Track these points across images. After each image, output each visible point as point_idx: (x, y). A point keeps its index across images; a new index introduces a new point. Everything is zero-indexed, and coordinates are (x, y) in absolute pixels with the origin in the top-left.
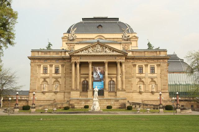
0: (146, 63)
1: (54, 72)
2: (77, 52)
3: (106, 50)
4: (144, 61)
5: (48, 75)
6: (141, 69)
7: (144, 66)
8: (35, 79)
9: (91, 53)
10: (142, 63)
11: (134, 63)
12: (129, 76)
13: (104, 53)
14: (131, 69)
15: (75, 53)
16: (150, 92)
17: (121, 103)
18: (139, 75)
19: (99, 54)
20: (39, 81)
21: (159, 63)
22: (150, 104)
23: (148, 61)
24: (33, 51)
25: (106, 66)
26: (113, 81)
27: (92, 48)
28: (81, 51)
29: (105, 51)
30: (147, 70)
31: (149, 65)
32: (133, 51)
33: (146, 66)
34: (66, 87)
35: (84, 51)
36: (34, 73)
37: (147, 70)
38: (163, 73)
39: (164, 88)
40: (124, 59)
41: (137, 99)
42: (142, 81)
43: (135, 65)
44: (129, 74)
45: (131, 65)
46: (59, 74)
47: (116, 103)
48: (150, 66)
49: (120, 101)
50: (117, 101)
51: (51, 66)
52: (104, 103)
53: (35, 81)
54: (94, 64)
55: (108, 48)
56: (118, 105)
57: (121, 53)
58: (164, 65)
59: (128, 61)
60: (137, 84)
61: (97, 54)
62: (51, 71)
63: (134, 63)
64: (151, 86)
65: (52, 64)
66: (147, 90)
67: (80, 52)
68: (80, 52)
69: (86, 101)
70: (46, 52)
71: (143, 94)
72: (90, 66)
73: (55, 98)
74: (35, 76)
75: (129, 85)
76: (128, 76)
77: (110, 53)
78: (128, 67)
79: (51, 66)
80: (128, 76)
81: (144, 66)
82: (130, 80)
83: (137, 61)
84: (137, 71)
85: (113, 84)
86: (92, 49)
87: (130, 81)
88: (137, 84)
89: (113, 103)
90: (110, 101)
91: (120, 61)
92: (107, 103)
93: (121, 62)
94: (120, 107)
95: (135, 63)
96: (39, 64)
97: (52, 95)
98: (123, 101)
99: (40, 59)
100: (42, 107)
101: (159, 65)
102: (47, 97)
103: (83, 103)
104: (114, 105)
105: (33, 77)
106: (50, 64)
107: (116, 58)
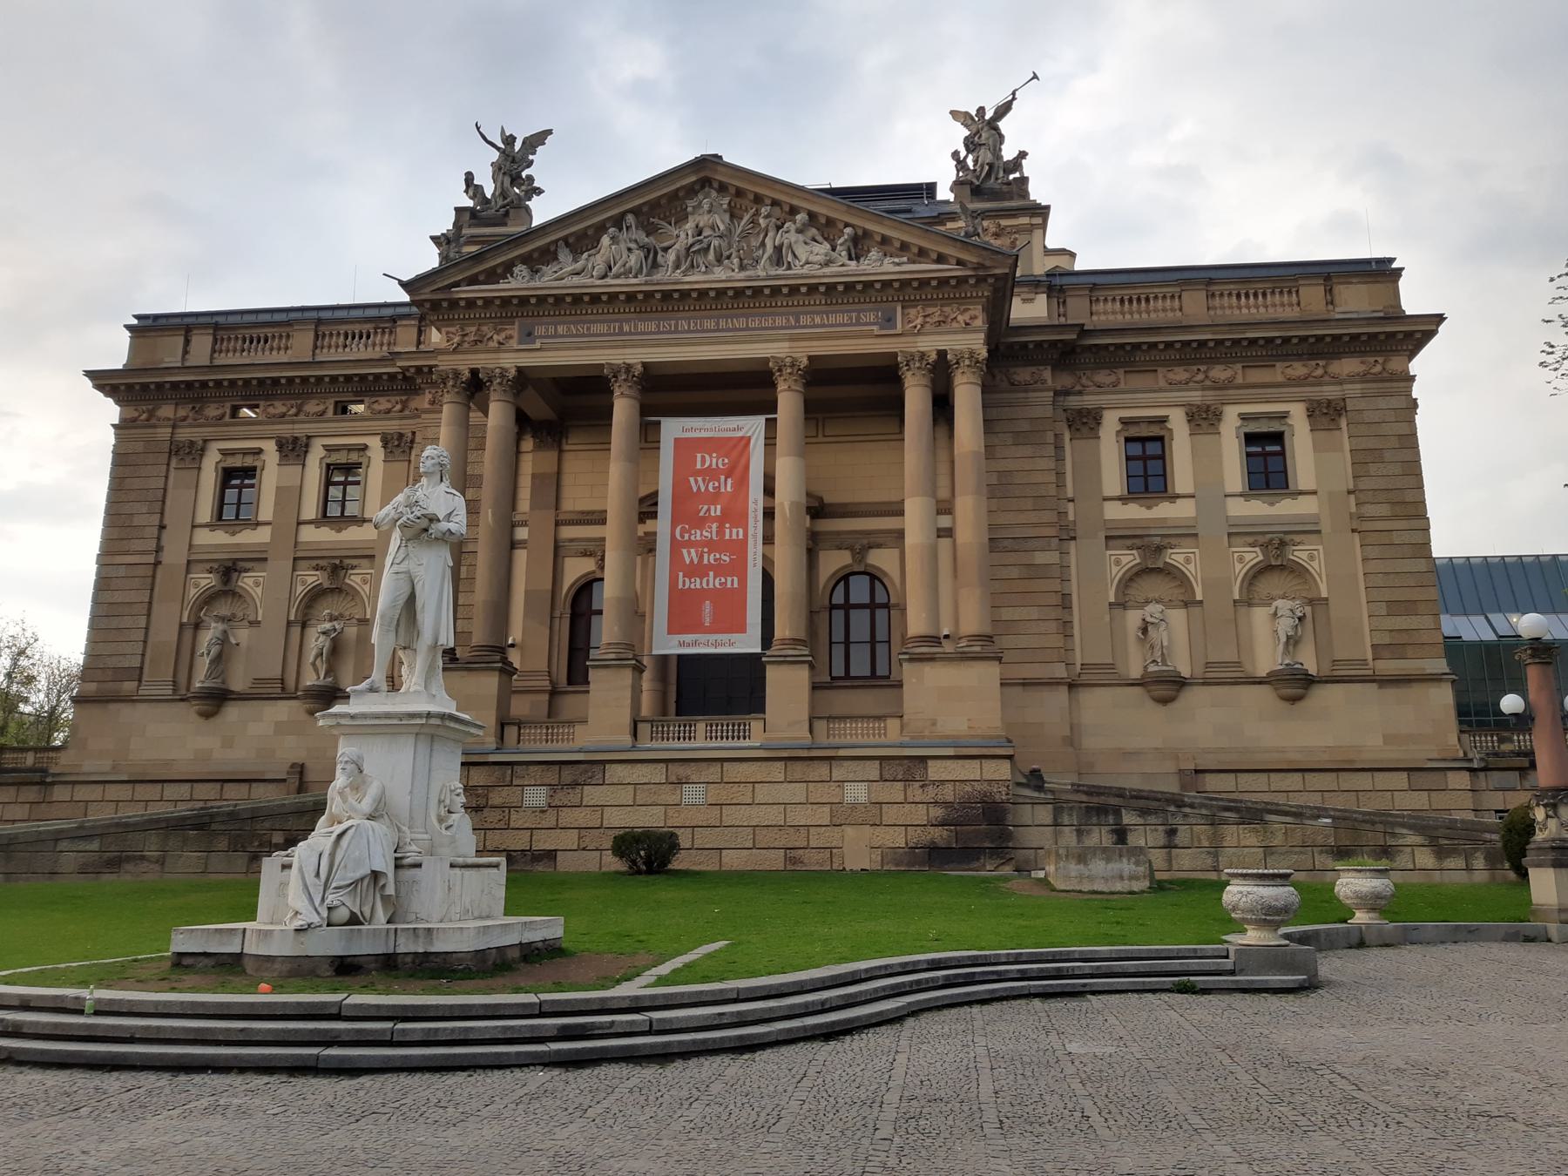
0: (1195, 397)
1: (310, 510)
2: (492, 276)
3: (790, 236)
4: (1180, 374)
5: (262, 536)
6: (1148, 467)
7: (1178, 422)
8: (141, 571)
9: (626, 274)
10: (1164, 401)
11: (1074, 402)
12: (1033, 517)
13: (763, 273)
14: (1051, 450)
15: (473, 280)
16: (1260, 682)
17: (948, 794)
18: (1135, 512)
19: (722, 276)
21: (1330, 392)
22: (1296, 801)
23: (1219, 373)
24: (147, 328)
25: (788, 402)
26: (874, 577)
27: (651, 230)
28: (526, 260)
29: (778, 249)
30: (1208, 464)
31: (1231, 414)
32: (1062, 289)
33: (1204, 419)
35: (564, 255)
36: (137, 521)
37: (1208, 464)
38: (1382, 483)
39: (1404, 638)
40: (979, 322)
41: (1127, 755)
42: (1169, 572)
43: (1085, 422)
44: (1029, 504)
45: (1048, 411)
46: (360, 521)
47: (895, 791)
48: (1244, 417)
49: (935, 771)
50: (907, 767)
51: (293, 450)
52: (762, 793)
53: (133, 597)
54: (671, 391)
55: (801, 217)
56: (920, 814)
57: (941, 259)
58: (1382, 403)
59: (1023, 374)
60: (1121, 605)
61: (696, 279)
62: (290, 496)
63: (1074, 402)
64: (1260, 614)
65: (300, 430)
66: (1229, 655)
67: (520, 269)
68: (520, 269)
69: (568, 775)
70: (255, 332)
71: (1194, 697)
72: (623, 409)
73: (299, 756)
74: (137, 545)
75: (1034, 613)
76: (1022, 518)
77: (833, 269)
78: (1020, 438)
79: (293, 450)
80: (1022, 518)
81: (1178, 422)
82: (1041, 558)
83: (1103, 377)
84: (1113, 476)
85: (872, 606)
86: (642, 237)
87: (1036, 572)
88: (1121, 605)
89: (857, 793)
90: (822, 770)
91: (930, 344)
92: (797, 792)
93: (942, 354)
94: (939, 835)
95: (1089, 401)
96: (184, 434)
97: (281, 728)
98: (970, 770)
99: (194, 392)
100: (95, 845)
101: (1325, 414)
102: (228, 743)
103: (536, 796)
104: (873, 815)
105: (127, 553)
106: (286, 430)
107: (889, 321)
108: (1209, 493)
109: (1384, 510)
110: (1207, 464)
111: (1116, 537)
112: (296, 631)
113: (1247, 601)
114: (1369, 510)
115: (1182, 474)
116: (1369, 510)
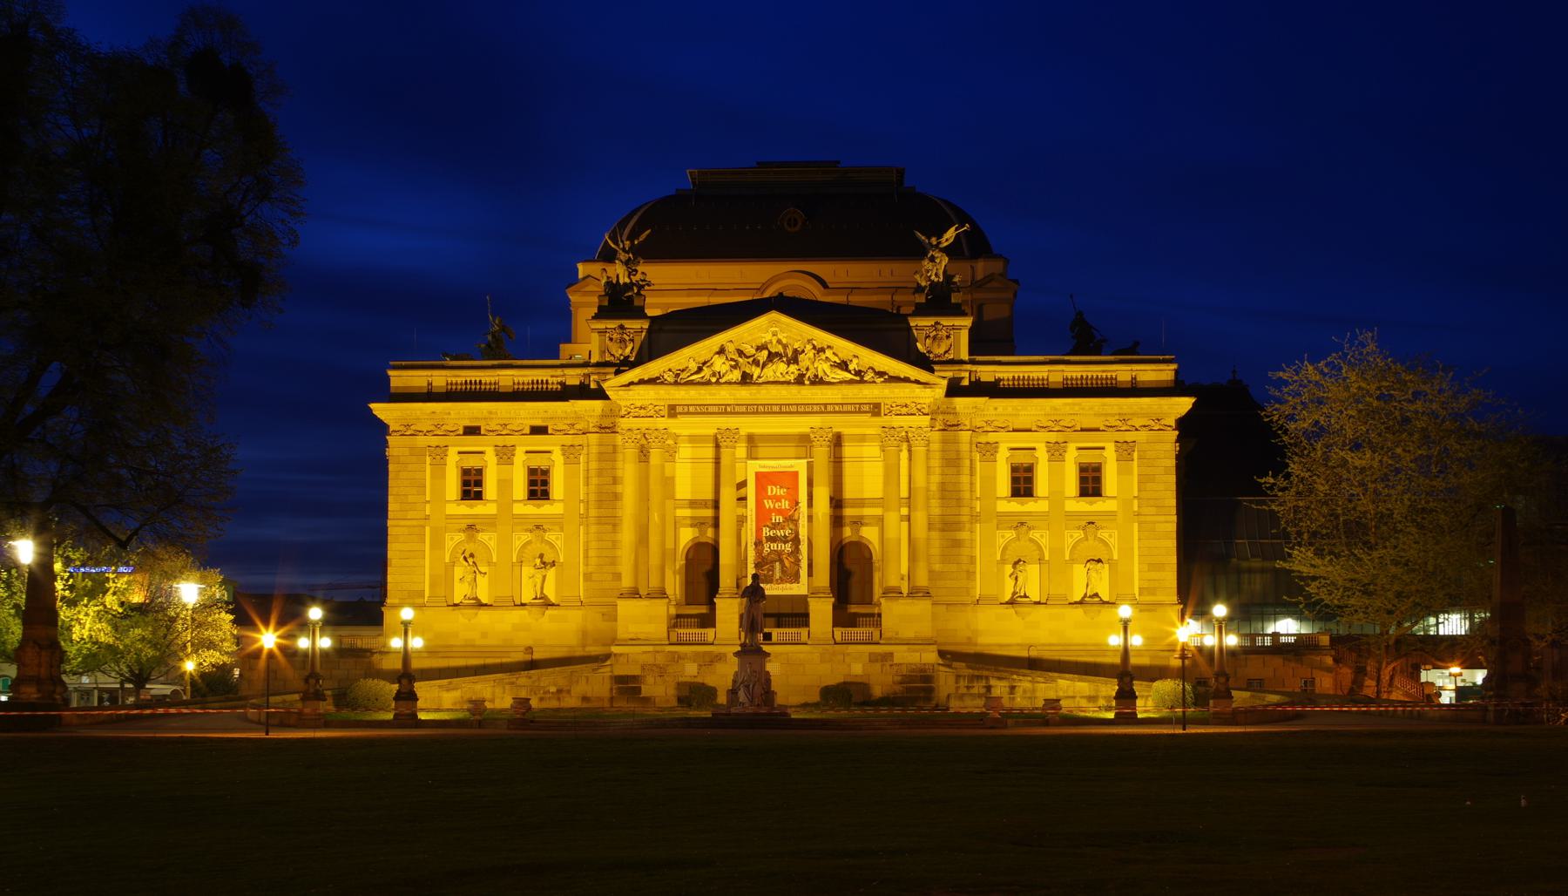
7: (1042, 454)
18: (1016, 506)
20: (438, 544)
21: (1130, 437)
31: (1072, 447)
33: (1056, 452)
34: (595, 577)
36: (411, 499)
43: (989, 450)
62: (505, 485)
81: (1042, 454)
84: (1004, 485)
101: (1125, 450)
108: (1056, 498)
109: (1153, 510)
110: (1056, 478)
111: (1003, 520)
112: (517, 569)
113: (1073, 560)
114: (1145, 510)
115: (1042, 484)
116: (1145, 510)
